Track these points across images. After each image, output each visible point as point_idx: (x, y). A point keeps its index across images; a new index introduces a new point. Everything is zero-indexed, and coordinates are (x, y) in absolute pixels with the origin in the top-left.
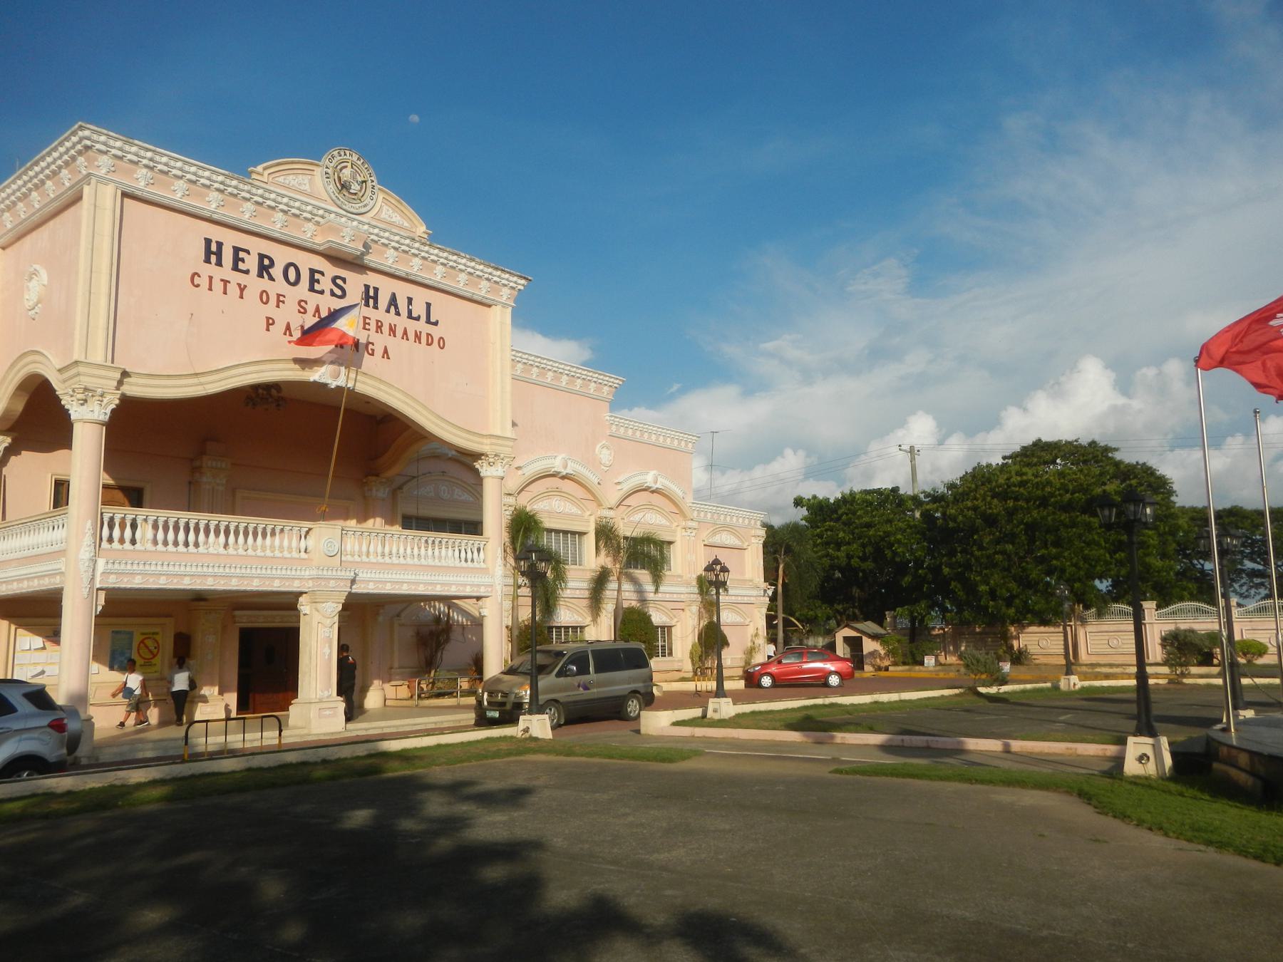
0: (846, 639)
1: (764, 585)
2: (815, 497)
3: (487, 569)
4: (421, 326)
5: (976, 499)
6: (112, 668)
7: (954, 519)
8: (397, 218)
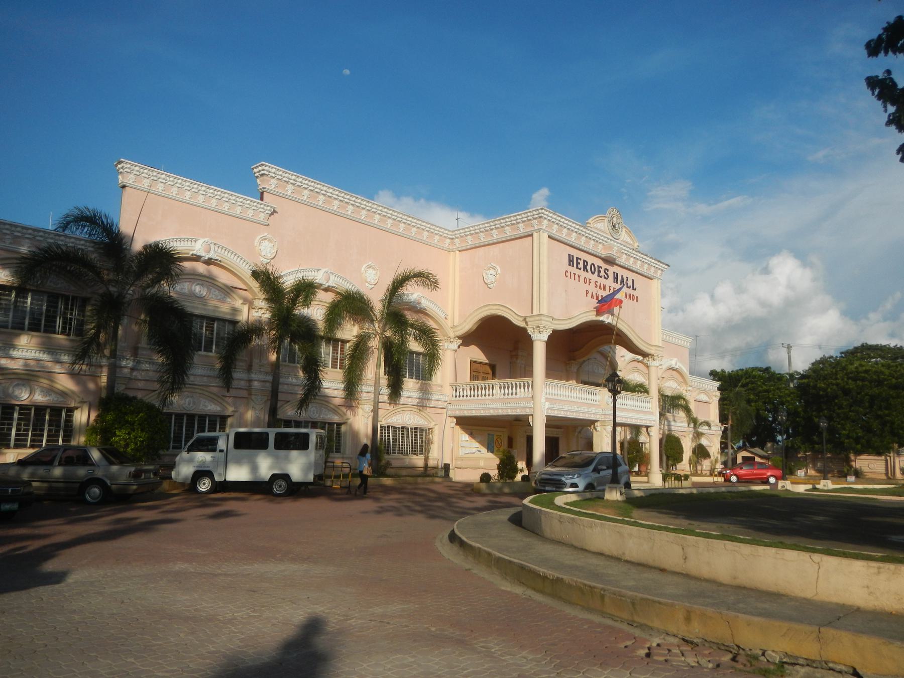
0: (744, 458)
1: (720, 424)
2: (723, 371)
4: (630, 291)
5: (836, 379)
7: (824, 390)
8: (629, 240)
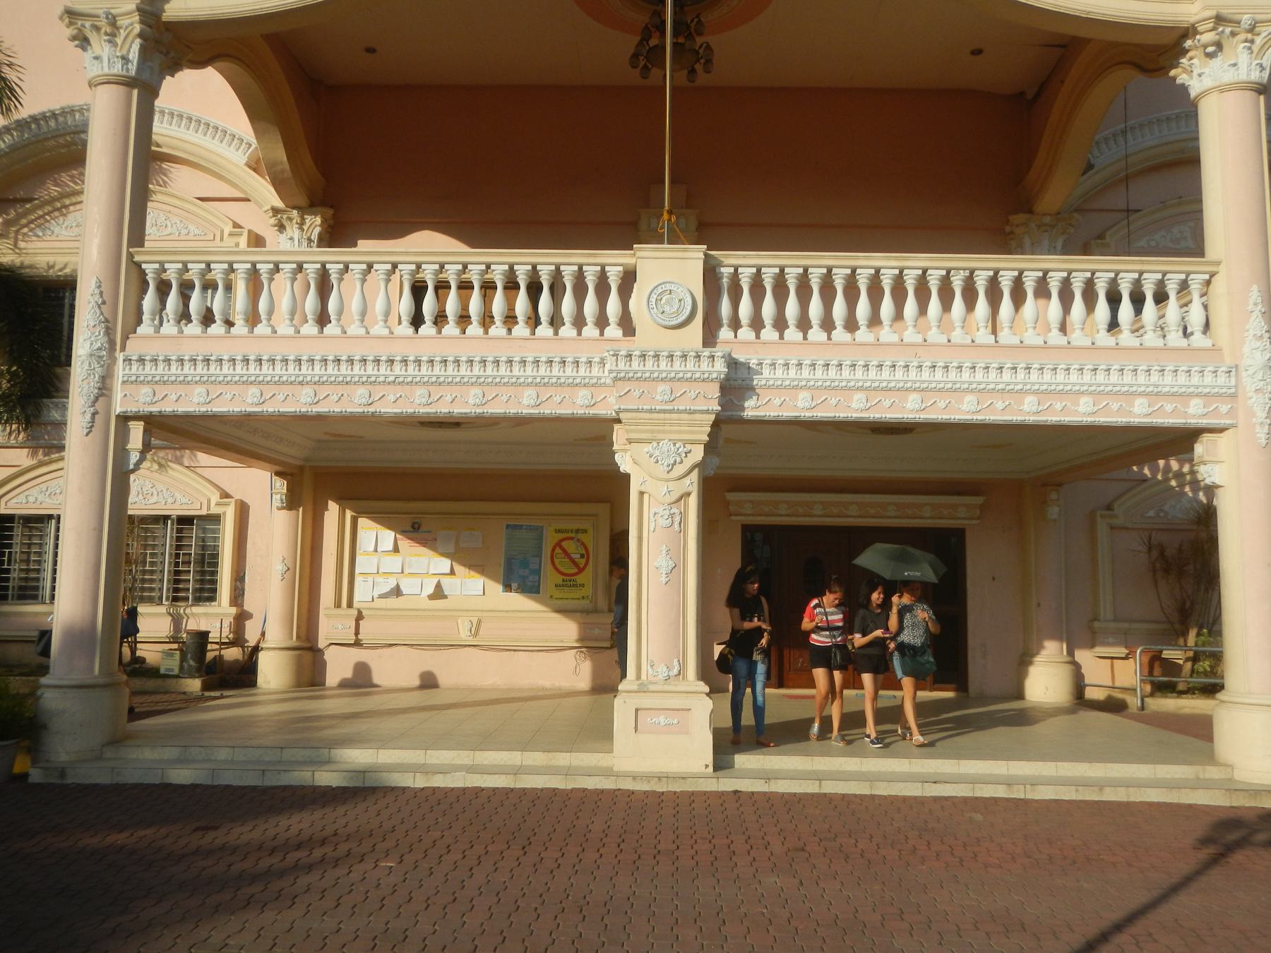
3: (1215, 349)
6: (508, 587)
